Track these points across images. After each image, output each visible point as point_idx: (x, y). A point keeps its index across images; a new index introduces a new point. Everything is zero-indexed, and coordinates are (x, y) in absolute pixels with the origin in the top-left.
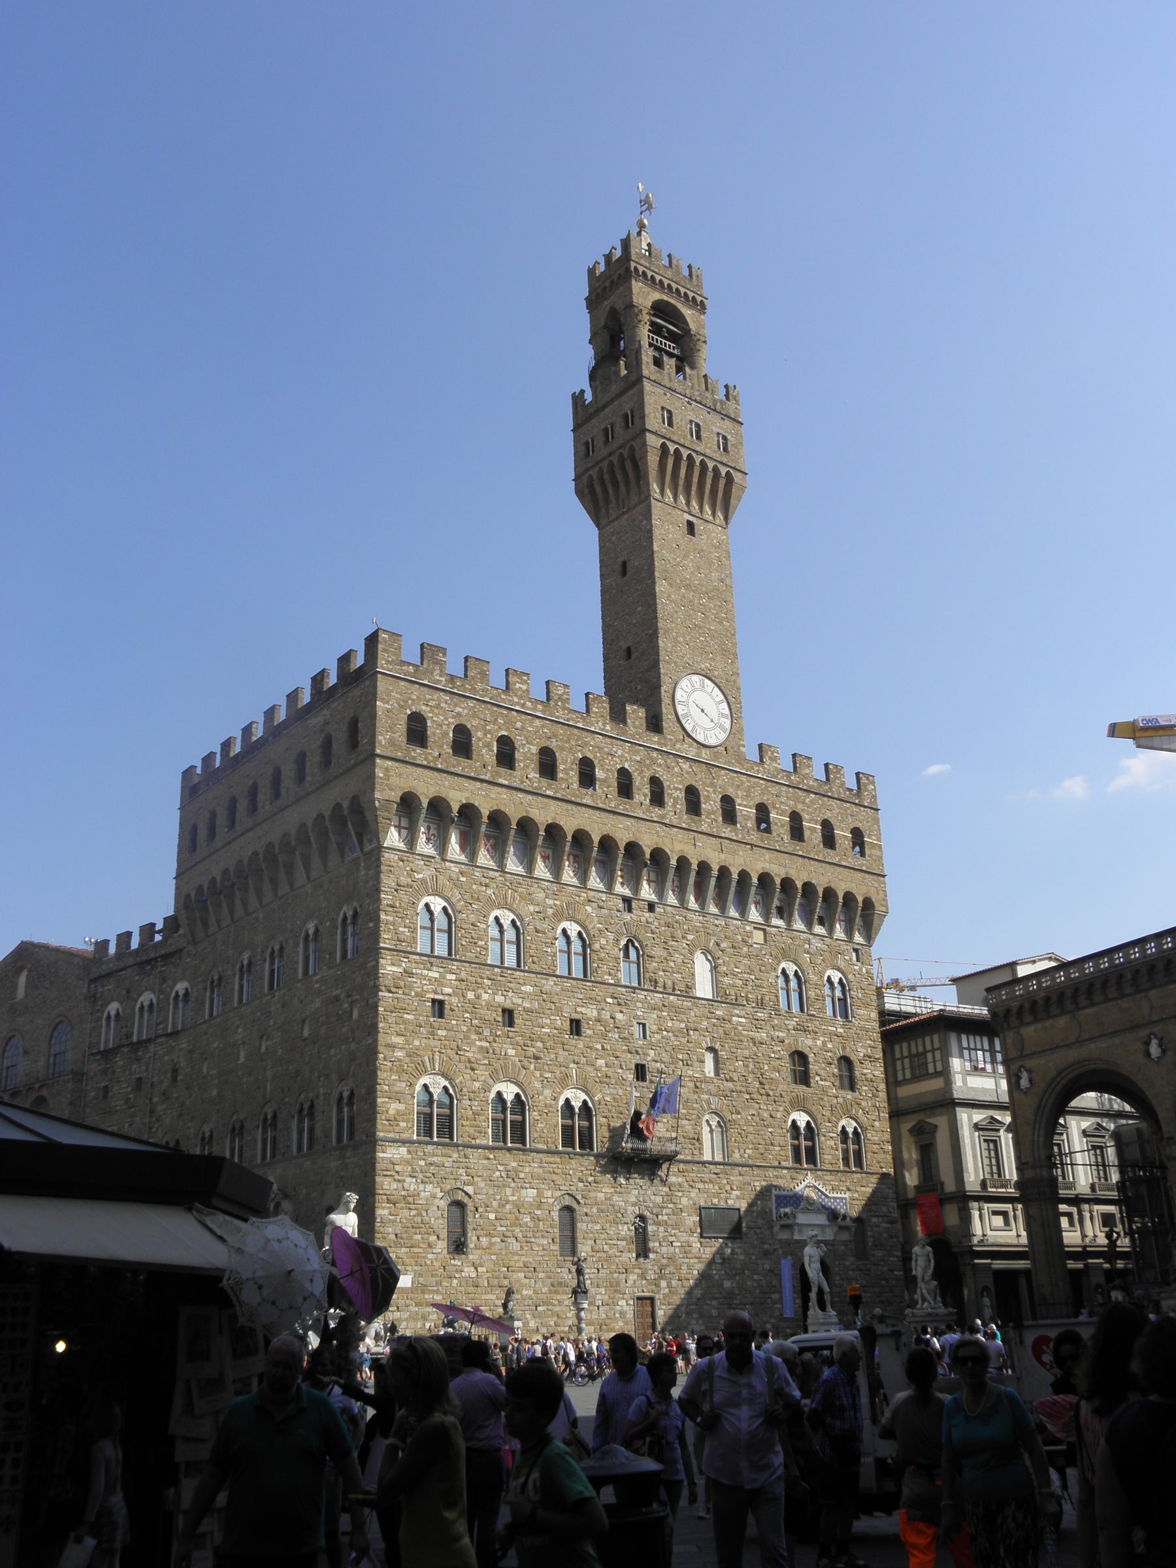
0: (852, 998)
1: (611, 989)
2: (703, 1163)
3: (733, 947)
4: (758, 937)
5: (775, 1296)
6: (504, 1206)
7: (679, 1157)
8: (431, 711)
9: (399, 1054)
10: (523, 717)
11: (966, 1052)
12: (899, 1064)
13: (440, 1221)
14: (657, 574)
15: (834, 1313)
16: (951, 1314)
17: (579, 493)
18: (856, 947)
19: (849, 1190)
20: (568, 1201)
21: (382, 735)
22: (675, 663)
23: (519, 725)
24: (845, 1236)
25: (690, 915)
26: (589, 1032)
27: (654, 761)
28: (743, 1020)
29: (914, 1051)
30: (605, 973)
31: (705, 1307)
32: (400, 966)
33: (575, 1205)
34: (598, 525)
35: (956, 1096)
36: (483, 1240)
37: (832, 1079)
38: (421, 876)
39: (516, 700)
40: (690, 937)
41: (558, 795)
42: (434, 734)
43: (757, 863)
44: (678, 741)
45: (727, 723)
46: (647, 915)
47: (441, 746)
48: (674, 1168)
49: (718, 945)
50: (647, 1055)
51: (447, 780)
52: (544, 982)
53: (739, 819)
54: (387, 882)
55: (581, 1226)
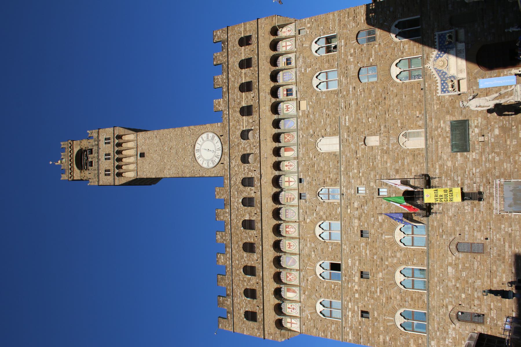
0: (324, 34)
1: (343, 210)
2: (427, 149)
4: (304, 105)
6: (457, 288)
8: (242, 307)
9: (388, 339)
13: (467, 327)
17: (154, 184)
18: (297, 32)
20: (453, 247)
21: (256, 334)
22: (193, 167)
23: (237, 262)
24: (462, 33)
25: (301, 156)
26: (366, 226)
27: (235, 183)
28: (347, 117)
30: (336, 212)
31: (511, 150)
32: (348, 332)
33: (456, 242)
36: (476, 302)
39: (228, 262)
40: (311, 155)
43: (268, 117)
44: (224, 167)
45: (211, 135)
46: (305, 183)
47: (254, 305)
50: (373, 187)
52: (345, 252)
53: (250, 128)
54: (314, 332)
55: (467, 238)
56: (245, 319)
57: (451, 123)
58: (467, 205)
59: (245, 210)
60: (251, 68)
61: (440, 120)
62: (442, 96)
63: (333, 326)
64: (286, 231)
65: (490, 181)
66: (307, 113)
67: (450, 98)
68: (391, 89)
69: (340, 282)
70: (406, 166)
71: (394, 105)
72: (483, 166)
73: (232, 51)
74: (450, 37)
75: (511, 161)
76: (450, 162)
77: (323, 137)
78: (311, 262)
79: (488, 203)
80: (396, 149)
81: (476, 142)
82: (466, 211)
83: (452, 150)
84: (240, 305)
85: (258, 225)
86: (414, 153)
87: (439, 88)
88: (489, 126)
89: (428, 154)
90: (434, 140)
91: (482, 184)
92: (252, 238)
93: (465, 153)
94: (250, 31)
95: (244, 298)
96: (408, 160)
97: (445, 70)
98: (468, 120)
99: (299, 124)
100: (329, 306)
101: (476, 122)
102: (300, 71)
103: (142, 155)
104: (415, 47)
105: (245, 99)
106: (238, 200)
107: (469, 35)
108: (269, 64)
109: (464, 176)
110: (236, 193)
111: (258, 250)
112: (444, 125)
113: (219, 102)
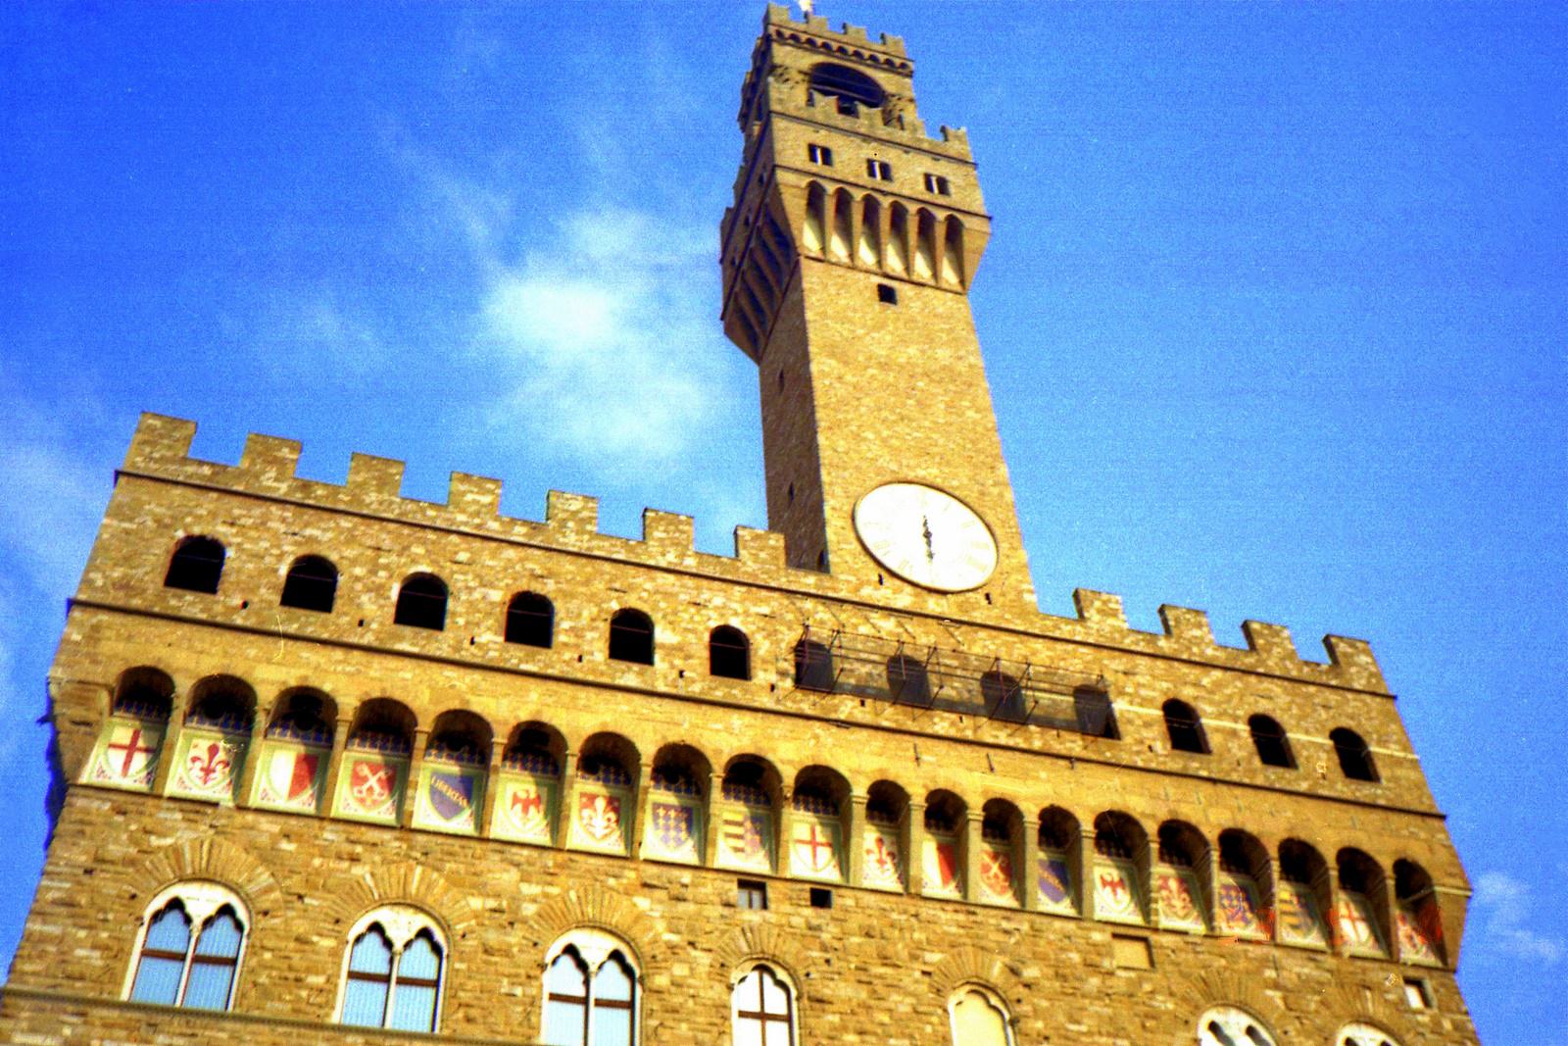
3: (1064, 978)
4: (1132, 954)
8: (243, 535)
10: (477, 544)
14: (813, 349)
18: (1412, 973)
23: (463, 556)
25: (927, 910)
34: (756, 355)
38: (169, 841)
39: (461, 517)
40: (934, 957)
41: (550, 672)
42: (239, 571)
44: (868, 582)
46: (809, 912)
47: (254, 590)
49: (1014, 972)
51: (253, 647)
56: (180, 534)
59: (693, 631)
60: (1257, 762)
63: (96, 959)
64: (592, 798)
66: (1106, 963)
69: (335, 1018)
73: (1310, 696)
77: (1013, 1022)
78: (446, 891)
84: (255, 527)
85: (630, 675)
92: (572, 640)
94: (1395, 779)
95: (292, 552)
99: (1058, 924)
100: (202, 950)
102: (1265, 962)
103: (887, 295)
105: (1140, 716)
106: (736, 614)
108: (1285, 836)
110: (766, 610)
111: (518, 655)
113: (1114, 614)
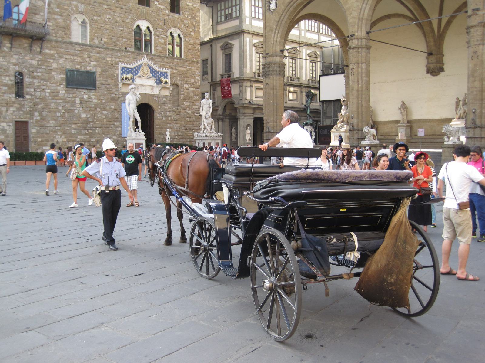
5: (118, 124)
7: (48, 37)
11: (253, 8)
12: (219, 13)
15: (144, 134)
16: (219, 136)
19: (172, 68)
24: (167, 93)
29: (227, 6)
31: (66, 128)
35: (245, 28)
37: (166, 5)
48: (45, 44)
57: (94, 73)
58: (10, 80)
61: (98, 62)
62: (118, 66)
65: (36, 106)
67: (116, 75)
68: (129, 17)
70: (53, 16)
71: (115, 17)
72: (52, 101)
74: (166, 83)
75: (57, 128)
76: (56, 67)
79: (14, 103)
80: (72, 9)
81: (75, 95)
82: (3, 78)
83: (68, 70)
86: (67, 29)
87: (126, 66)
88: (89, 109)
89: (65, 44)
90: (79, 52)
91: (33, 97)
93: (64, 83)
96: (60, 19)
97: (139, 74)
98: (95, 90)
101: (93, 97)
104: (160, 49)
107: (164, 99)
109: (42, 79)
112: (92, 65)
